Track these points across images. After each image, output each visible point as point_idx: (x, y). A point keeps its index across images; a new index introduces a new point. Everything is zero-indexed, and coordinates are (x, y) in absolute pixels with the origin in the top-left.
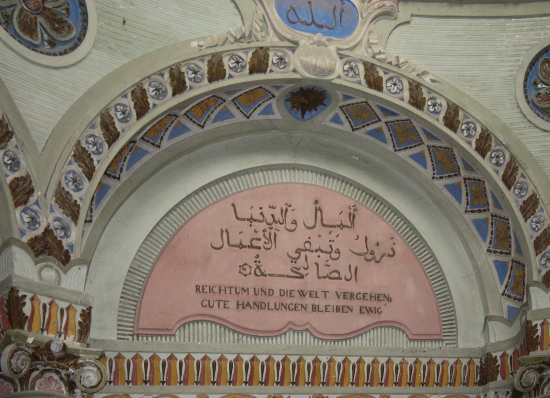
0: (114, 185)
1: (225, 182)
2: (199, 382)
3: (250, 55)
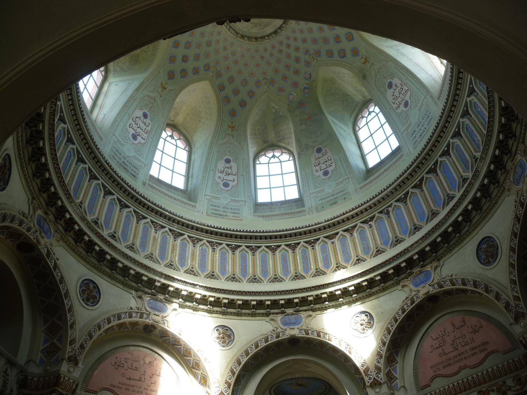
3: (410, 301)
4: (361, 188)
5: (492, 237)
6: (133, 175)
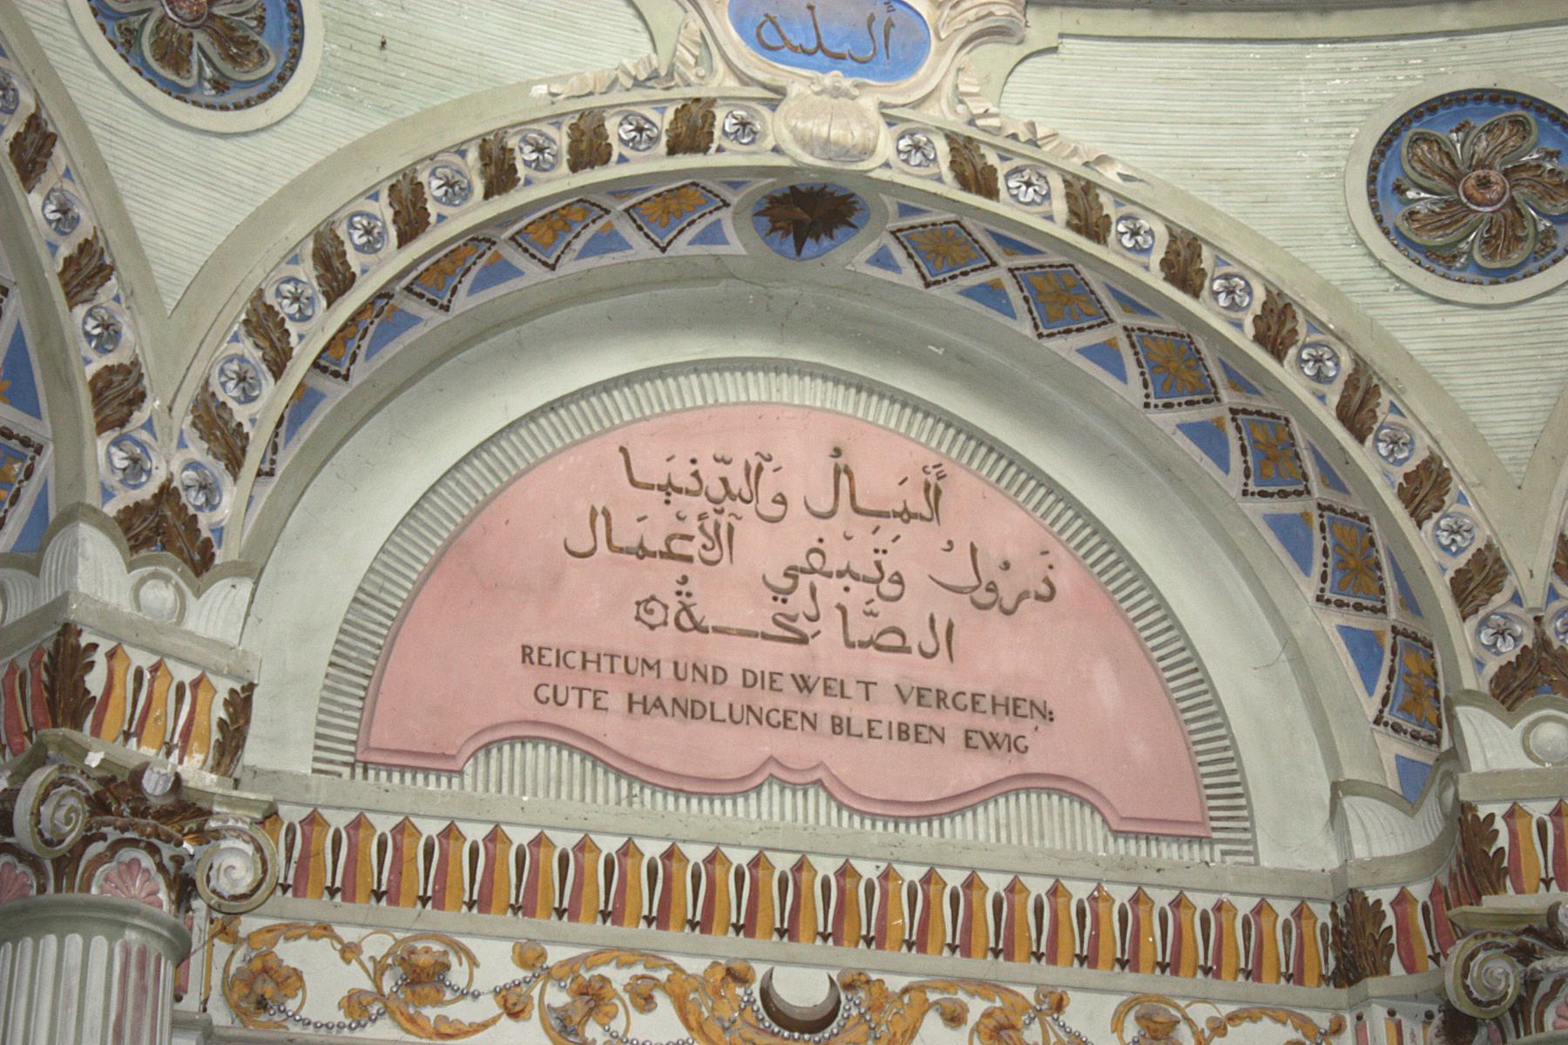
0: (335, 391)
1: (604, 396)
2: (520, 908)
3: (670, 114)
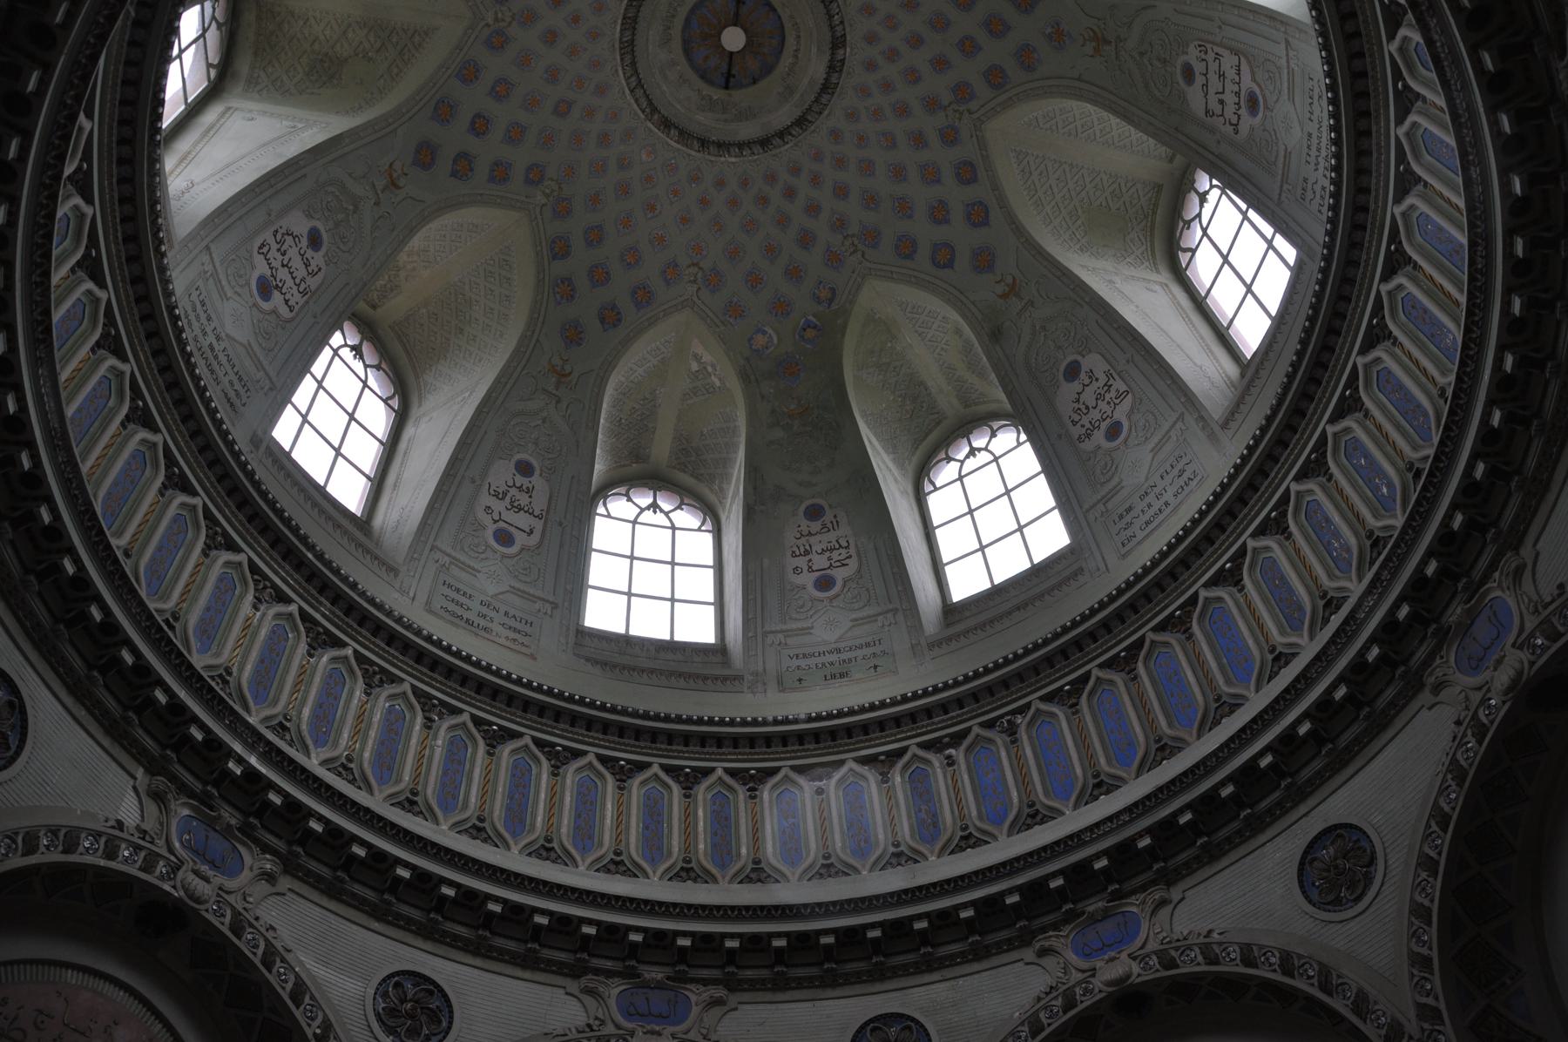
3: (1060, 999)
4: (933, 646)
5: (1356, 827)
6: (229, 400)
